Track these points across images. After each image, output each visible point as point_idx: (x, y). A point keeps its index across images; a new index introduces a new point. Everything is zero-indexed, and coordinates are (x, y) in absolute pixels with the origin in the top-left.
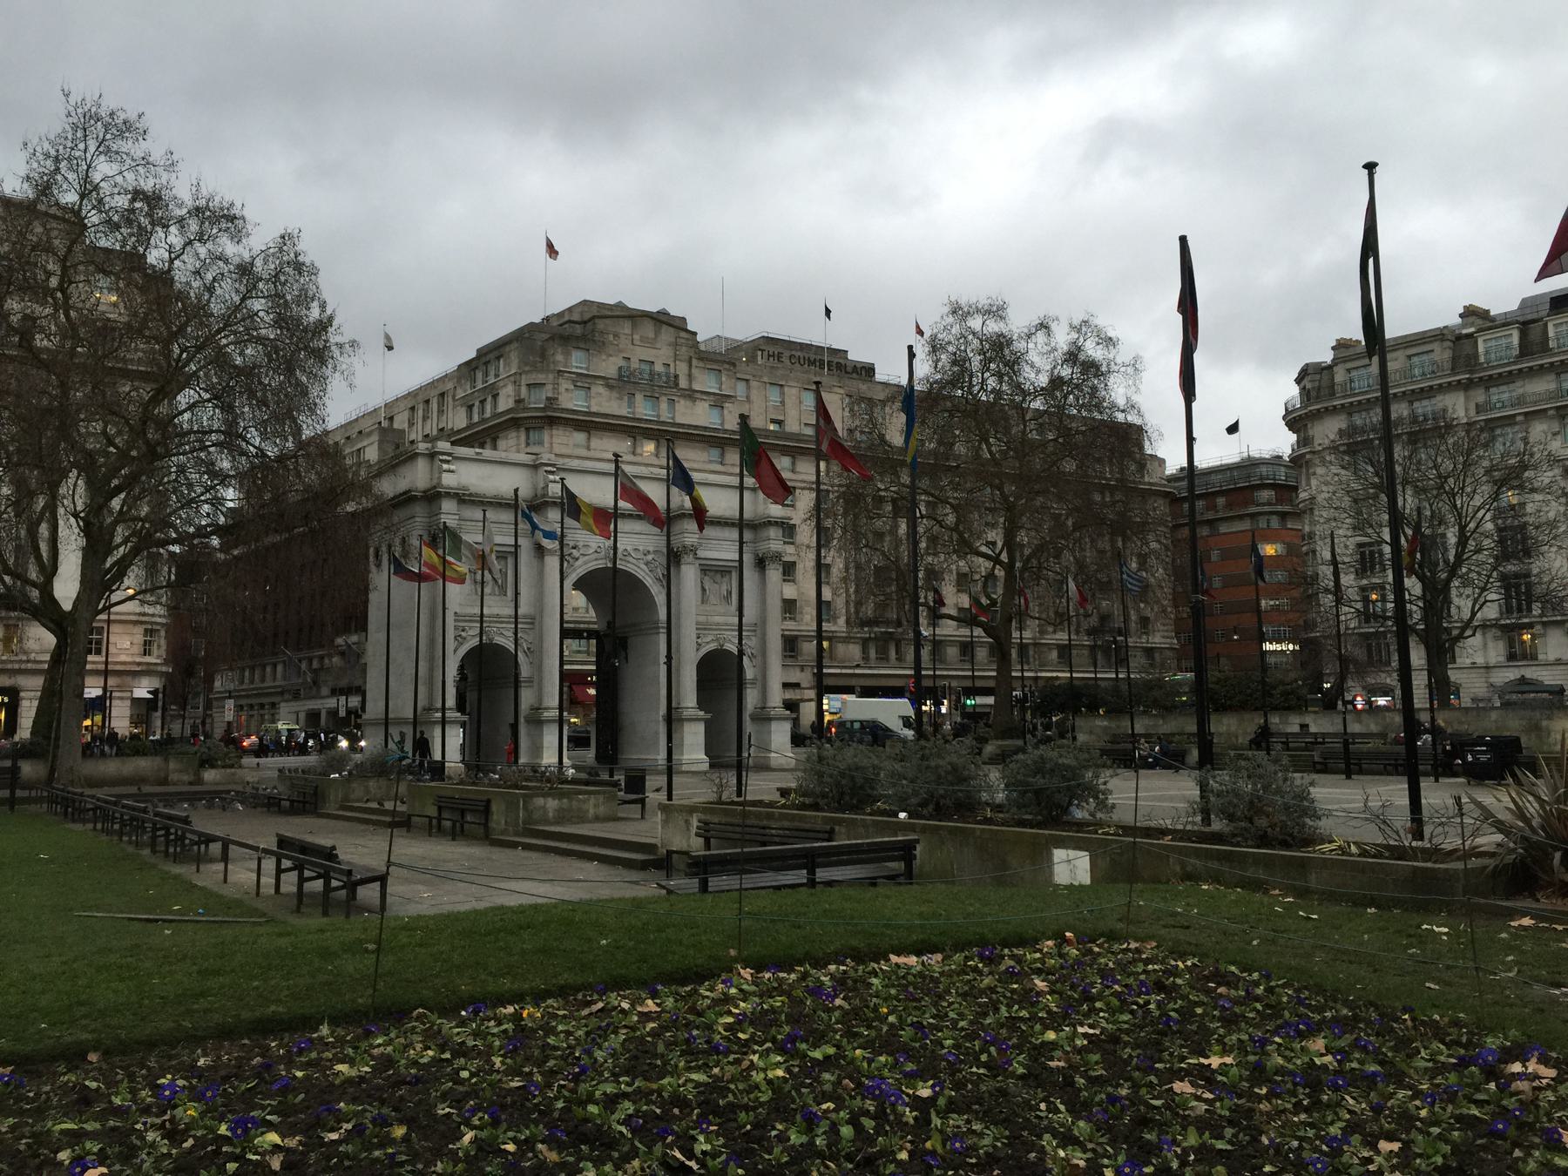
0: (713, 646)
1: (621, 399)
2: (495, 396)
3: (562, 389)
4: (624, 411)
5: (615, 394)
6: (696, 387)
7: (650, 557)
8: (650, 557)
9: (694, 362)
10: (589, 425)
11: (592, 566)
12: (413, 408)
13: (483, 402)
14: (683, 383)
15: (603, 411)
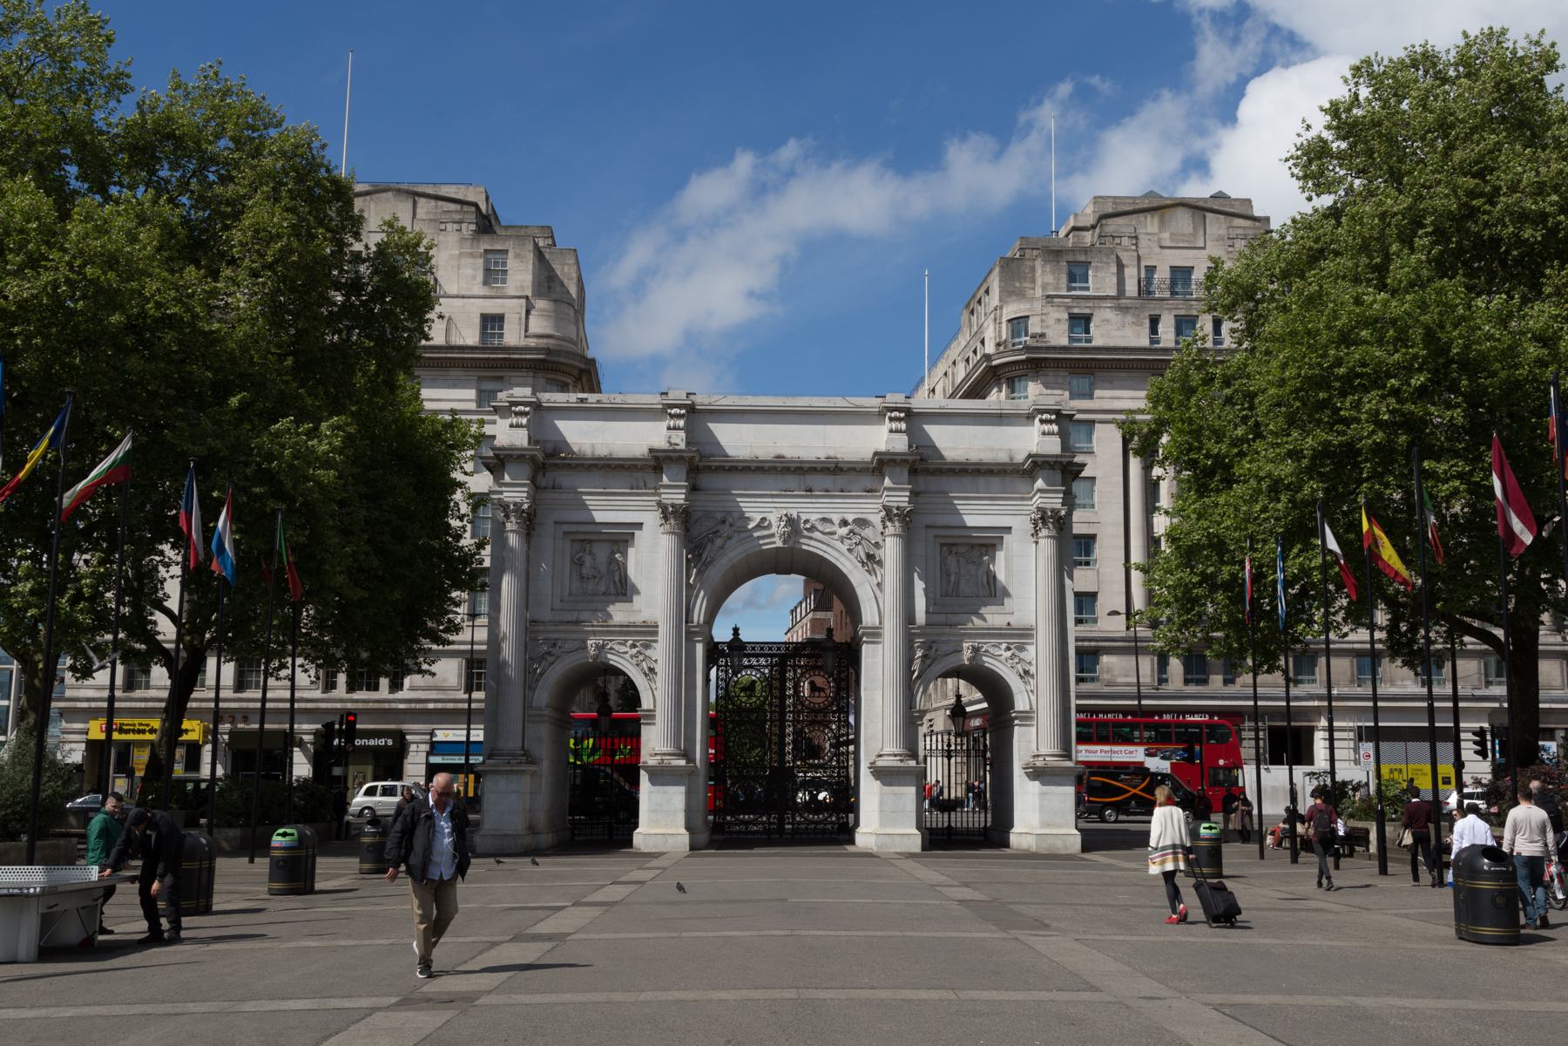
1: (1139, 324)
2: (983, 342)
3: (1051, 322)
4: (1145, 342)
5: (1129, 318)
8: (844, 531)
13: (975, 352)
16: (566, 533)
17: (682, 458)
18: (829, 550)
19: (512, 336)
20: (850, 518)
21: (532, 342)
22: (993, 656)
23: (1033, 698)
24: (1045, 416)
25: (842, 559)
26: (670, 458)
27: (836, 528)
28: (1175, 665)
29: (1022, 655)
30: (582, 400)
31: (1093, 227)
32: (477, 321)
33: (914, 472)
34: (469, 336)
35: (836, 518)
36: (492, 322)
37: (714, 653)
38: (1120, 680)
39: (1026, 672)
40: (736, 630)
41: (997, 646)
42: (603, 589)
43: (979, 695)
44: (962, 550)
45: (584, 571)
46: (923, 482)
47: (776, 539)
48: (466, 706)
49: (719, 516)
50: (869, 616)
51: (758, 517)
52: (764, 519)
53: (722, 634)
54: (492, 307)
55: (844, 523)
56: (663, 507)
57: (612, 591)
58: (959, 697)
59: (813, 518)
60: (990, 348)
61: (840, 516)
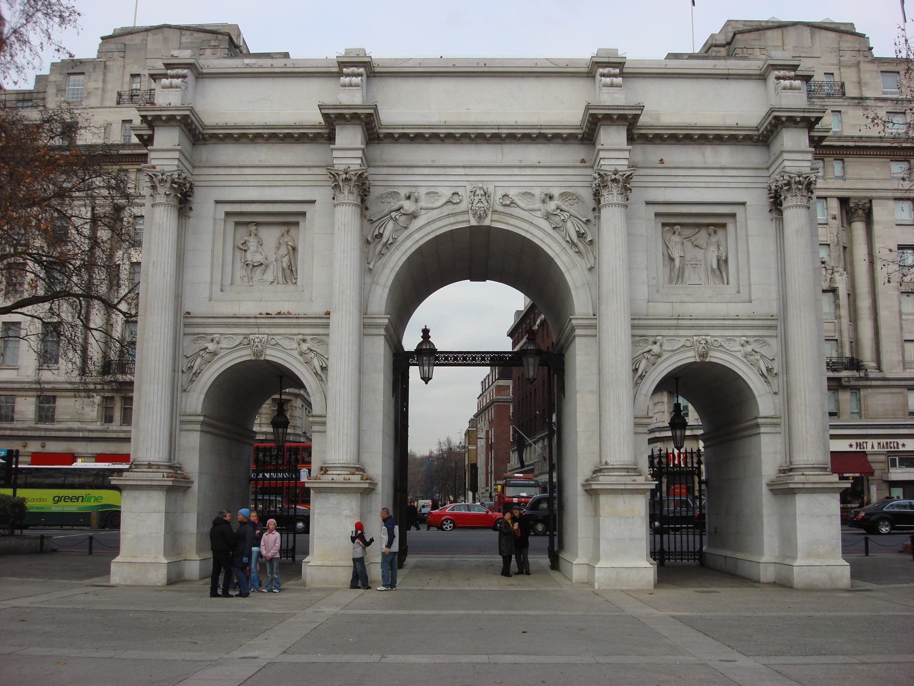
0: (689, 357)
6: (867, 94)
8: (552, 206)
9: (862, 66)
14: (851, 91)
16: (228, 214)
17: (355, 117)
20: (556, 192)
22: (728, 352)
23: (778, 399)
24: (782, 73)
25: (547, 240)
29: (764, 351)
31: (729, 44)
33: (631, 139)
35: (537, 192)
39: (769, 370)
40: (426, 332)
41: (730, 339)
44: (687, 232)
49: (403, 192)
50: (580, 304)
51: (447, 193)
53: (411, 341)
55: (551, 198)
56: (334, 176)
59: (512, 193)
61: (547, 191)
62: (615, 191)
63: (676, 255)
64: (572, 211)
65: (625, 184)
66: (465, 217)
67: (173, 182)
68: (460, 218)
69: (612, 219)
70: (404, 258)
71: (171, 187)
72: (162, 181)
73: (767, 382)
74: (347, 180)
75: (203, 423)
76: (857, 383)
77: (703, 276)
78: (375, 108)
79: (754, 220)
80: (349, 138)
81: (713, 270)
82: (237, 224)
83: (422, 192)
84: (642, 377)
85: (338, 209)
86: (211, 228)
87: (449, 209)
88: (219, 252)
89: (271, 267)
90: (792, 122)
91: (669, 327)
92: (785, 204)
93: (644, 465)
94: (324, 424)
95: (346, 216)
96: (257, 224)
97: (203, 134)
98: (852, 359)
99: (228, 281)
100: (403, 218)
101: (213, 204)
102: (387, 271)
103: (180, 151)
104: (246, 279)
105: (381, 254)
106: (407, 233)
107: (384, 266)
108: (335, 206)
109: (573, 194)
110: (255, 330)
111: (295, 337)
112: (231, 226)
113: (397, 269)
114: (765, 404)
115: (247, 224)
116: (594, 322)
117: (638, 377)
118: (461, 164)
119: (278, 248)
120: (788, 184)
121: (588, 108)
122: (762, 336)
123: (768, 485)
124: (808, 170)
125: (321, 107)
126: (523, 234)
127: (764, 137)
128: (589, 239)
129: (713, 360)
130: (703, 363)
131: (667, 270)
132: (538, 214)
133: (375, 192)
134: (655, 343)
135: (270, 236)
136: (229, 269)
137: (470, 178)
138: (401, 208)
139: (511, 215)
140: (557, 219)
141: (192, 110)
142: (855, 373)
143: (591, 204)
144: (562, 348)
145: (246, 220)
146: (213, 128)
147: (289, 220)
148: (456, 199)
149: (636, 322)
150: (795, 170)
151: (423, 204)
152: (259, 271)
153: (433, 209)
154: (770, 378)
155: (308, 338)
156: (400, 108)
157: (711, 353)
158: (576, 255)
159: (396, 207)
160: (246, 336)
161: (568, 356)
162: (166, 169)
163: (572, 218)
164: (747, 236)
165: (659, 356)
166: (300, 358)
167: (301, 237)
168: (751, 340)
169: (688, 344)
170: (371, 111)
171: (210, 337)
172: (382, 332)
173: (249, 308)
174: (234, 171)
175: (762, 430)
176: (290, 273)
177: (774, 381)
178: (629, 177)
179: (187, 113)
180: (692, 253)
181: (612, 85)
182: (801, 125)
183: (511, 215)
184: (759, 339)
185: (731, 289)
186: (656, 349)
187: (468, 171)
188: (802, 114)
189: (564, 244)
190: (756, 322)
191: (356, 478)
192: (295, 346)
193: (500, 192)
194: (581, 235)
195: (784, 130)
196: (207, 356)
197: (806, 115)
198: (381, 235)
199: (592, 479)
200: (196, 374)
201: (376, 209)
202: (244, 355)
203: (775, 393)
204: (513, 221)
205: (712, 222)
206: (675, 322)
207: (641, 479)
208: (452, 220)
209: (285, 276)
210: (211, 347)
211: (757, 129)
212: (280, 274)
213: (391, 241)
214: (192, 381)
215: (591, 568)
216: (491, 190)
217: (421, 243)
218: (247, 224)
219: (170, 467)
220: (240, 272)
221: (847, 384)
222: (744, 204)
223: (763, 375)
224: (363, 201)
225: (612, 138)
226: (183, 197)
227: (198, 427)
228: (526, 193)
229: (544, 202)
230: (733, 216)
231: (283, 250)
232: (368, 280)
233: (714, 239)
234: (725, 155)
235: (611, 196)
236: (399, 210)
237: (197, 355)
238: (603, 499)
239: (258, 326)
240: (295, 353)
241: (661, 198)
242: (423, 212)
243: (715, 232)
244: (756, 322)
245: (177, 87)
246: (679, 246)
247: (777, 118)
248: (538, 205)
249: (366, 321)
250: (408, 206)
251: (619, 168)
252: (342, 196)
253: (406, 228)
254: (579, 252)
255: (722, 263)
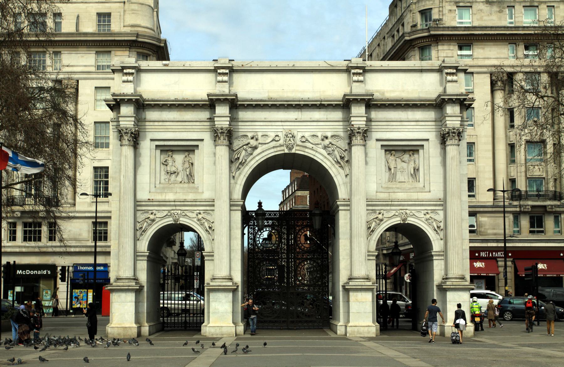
0: (397, 221)
1: (501, 12)
2: (403, 25)
3: (446, 11)
5: (495, 8)
7: (327, 142)
8: (327, 142)
10: (466, 39)
11: (271, 153)
12: (379, 45)
13: (398, 31)
15: (484, 24)
16: (156, 146)
18: (317, 154)
19: (116, 26)
20: (329, 135)
21: (128, 30)
23: (442, 242)
25: (325, 160)
26: (219, 100)
27: (320, 142)
28: (525, 222)
29: (436, 217)
30: (165, 65)
32: (95, 17)
34: (89, 26)
36: (104, 18)
37: (247, 217)
38: (490, 231)
39: (438, 227)
40: (260, 204)
41: (419, 211)
42: (180, 180)
43: (407, 240)
45: (169, 169)
46: (374, 114)
47: (284, 148)
48: (93, 250)
49: (250, 135)
50: (342, 193)
51: (272, 135)
52: (276, 136)
53: (252, 206)
54: (103, 8)
55: (327, 138)
57: (186, 181)
58: (396, 243)
59: (307, 135)
60: (408, 29)
61: (324, 135)
62: (359, 138)
63: (392, 167)
64: (337, 145)
65: (365, 134)
66: (282, 148)
67: (132, 133)
68: (279, 149)
69: (357, 152)
70: (251, 170)
71: (131, 136)
72: (126, 133)
73: (438, 233)
74: (222, 133)
75: (148, 257)
76: (558, 209)
77: (406, 177)
78: (236, 96)
79: (432, 148)
80: (222, 110)
81: (412, 175)
82: (161, 151)
83: (260, 134)
84: (373, 231)
85: (217, 147)
86: (149, 154)
87: (274, 144)
88: (153, 167)
89: (180, 174)
90: (452, 101)
91: (387, 205)
92: (447, 143)
93: (373, 275)
94: (213, 256)
95: (223, 151)
96: (172, 151)
97: (143, 104)
98: (555, 192)
99: (158, 182)
100: (250, 149)
101: (149, 141)
102: (242, 176)
103: (135, 117)
104: (167, 180)
105: (238, 168)
106: (251, 157)
107: (240, 174)
108: (216, 146)
109: (338, 136)
110: (174, 208)
111: (195, 212)
112: (158, 152)
113: (247, 176)
114: (437, 246)
115: (167, 151)
116: (349, 203)
117: (370, 231)
118: (280, 120)
119: (184, 164)
120: (448, 133)
121: (345, 95)
122: (435, 210)
123: (437, 286)
124: (459, 126)
125: (208, 95)
126: (312, 156)
127: (439, 104)
128: (346, 159)
129: (409, 222)
130: (404, 224)
131: (388, 174)
132: (320, 146)
133: (235, 135)
134: (380, 213)
135: (179, 158)
136: (158, 175)
137: (285, 127)
138: (249, 143)
139: (306, 147)
140: (330, 149)
141: (141, 96)
142: (557, 203)
143: (347, 141)
144: (334, 212)
145: (167, 149)
146: (148, 101)
147: (189, 149)
148: (277, 138)
149: (370, 203)
150: (451, 126)
151: (260, 141)
152: (174, 176)
153: (265, 144)
154: (439, 231)
155: (202, 212)
156: (247, 87)
157: (409, 219)
158: (340, 169)
159: (246, 143)
160: (169, 211)
161: (336, 217)
162: (128, 126)
163: (337, 149)
164: (429, 157)
165: (382, 220)
166: (198, 222)
167: (196, 158)
168: (429, 212)
169: (397, 214)
170: (234, 97)
171: (150, 212)
172: (240, 208)
173: (170, 196)
174: (160, 123)
175: (434, 258)
176: (190, 177)
177: (442, 234)
178: (366, 132)
179: (139, 98)
180: (400, 165)
181: (358, 81)
182: (456, 102)
183: (306, 147)
184: (433, 211)
185: (421, 185)
186: (380, 216)
187: (283, 124)
188: (456, 97)
189: (334, 162)
190: (432, 203)
191: (230, 284)
192: (194, 215)
193: (300, 135)
194: (342, 158)
195: (447, 105)
196: (149, 222)
197: (458, 97)
198: (239, 158)
199: (347, 283)
200: (144, 231)
201: (237, 144)
202: (169, 221)
203: (441, 239)
204: (307, 150)
205: (412, 149)
206: (390, 203)
207: (370, 283)
208: (275, 149)
209: (188, 179)
210: (152, 217)
211: (435, 100)
212: (185, 178)
213: (244, 161)
214: (141, 235)
215: (346, 326)
216: (295, 134)
217: (259, 162)
218: (167, 151)
219: (134, 279)
220: (164, 176)
221: (551, 210)
222: (428, 140)
223: (435, 230)
224: (230, 141)
225: (358, 111)
226: (135, 139)
227: (146, 258)
228: (313, 136)
229: (323, 140)
230: (423, 146)
231: (187, 165)
232: (232, 181)
233: (412, 158)
234: (419, 114)
235: (357, 140)
236: (247, 144)
237: (144, 220)
238: (351, 294)
239: (175, 206)
240: (195, 220)
241: (385, 138)
242: (260, 145)
243: (413, 154)
244: (432, 203)
245: (131, 82)
246: (394, 162)
247: (444, 99)
248: (320, 142)
249: (231, 203)
250: (253, 143)
251: (361, 126)
252: (220, 141)
253: (252, 154)
254: (341, 167)
255: (416, 170)
